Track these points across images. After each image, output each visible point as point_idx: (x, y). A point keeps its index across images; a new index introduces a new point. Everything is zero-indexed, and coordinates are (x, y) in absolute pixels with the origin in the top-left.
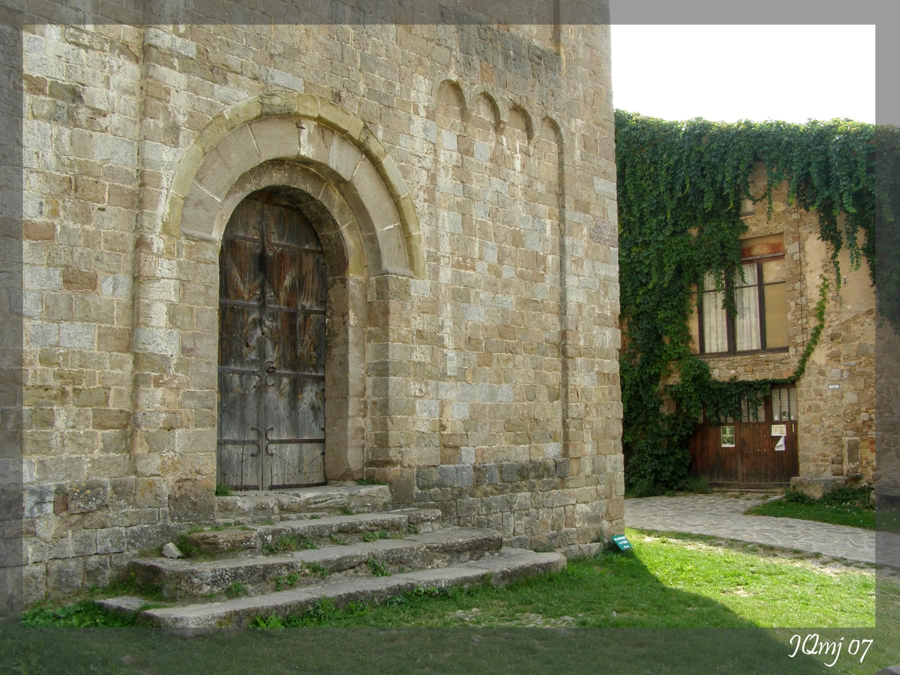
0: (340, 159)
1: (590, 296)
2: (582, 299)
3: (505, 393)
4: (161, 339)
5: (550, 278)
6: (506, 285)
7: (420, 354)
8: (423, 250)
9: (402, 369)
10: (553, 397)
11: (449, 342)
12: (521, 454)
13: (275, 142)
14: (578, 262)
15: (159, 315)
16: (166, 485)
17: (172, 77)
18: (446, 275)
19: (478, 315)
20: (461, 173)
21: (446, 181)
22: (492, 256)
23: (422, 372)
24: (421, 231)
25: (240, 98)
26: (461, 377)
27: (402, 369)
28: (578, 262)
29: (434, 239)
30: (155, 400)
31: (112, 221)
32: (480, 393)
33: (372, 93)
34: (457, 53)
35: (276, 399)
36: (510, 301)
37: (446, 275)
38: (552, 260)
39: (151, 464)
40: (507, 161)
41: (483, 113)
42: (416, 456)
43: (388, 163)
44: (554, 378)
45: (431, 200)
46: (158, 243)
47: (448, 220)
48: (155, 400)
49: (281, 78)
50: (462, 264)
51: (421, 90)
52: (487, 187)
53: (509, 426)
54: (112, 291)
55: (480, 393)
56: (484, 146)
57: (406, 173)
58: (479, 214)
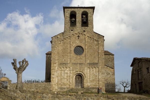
0: (81, 73)
1: (101, 77)
2: (100, 77)
3: (93, 84)
4: (71, 82)
5: (98, 77)
6: (93, 78)
7: (86, 82)
8: (86, 76)
9: (85, 82)
10: (98, 84)
11: (89, 81)
12: (95, 87)
13: (77, 73)
14: (100, 75)
15: (71, 81)
16: (71, 88)
17: (71, 71)
18: (88, 77)
19: (91, 79)
20: (90, 72)
21: (88, 73)
22: (92, 76)
23: (86, 83)
24: (86, 76)
25: (75, 71)
26: (89, 83)
27: (85, 82)
28: (100, 75)
29: (87, 76)
30: (70, 84)
31: (69, 77)
32: (91, 84)
33: (82, 69)
34: (89, 65)
35: (79, 84)
36: (94, 78)
37: (88, 77)
38: (98, 76)
39: (70, 87)
40: (94, 70)
41: (92, 68)
42: (85, 87)
43: (84, 73)
44: (98, 83)
45: (87, 74)
46: (71, 78)
47: (88, 75)
48: (70, 84)
49: (77, 70)
50: (90, 76)
51: (86, 68)
52: (91, 72)
53: (94, 85)
54: (69, 80)
55: (91, 84)
56: (91, 70)
57: (85, 73)
58: (91, 74)
